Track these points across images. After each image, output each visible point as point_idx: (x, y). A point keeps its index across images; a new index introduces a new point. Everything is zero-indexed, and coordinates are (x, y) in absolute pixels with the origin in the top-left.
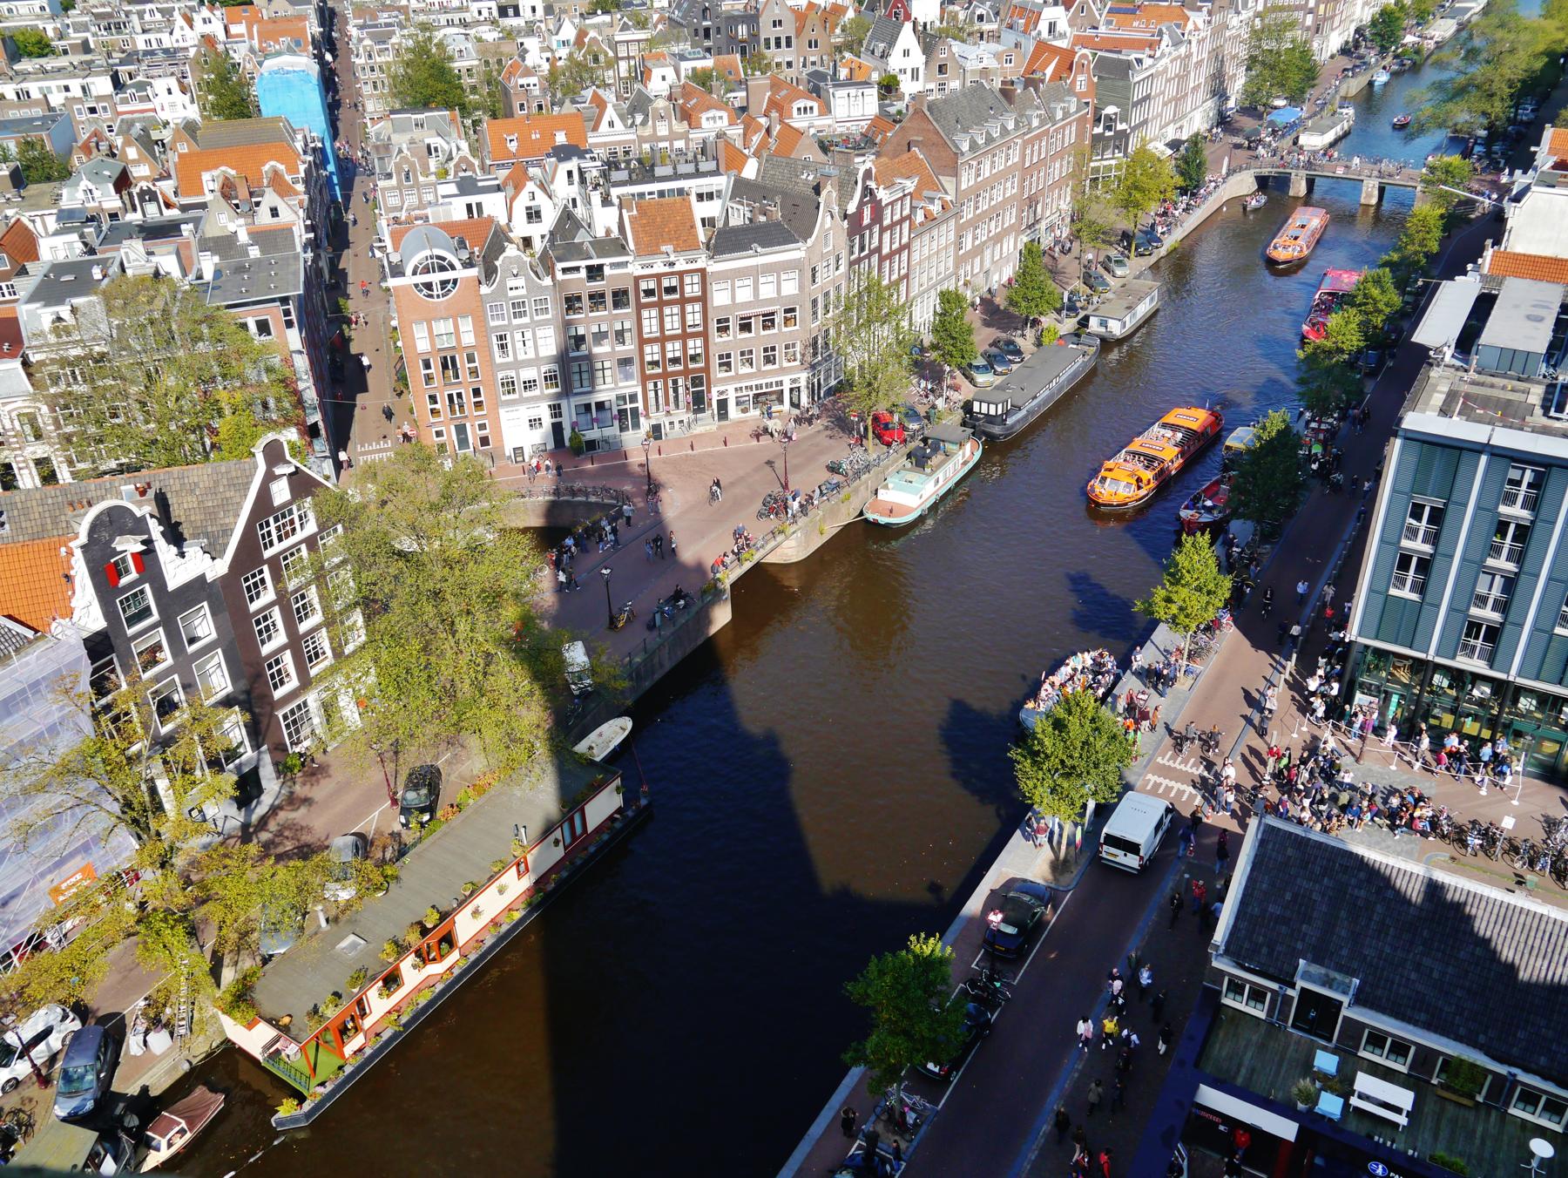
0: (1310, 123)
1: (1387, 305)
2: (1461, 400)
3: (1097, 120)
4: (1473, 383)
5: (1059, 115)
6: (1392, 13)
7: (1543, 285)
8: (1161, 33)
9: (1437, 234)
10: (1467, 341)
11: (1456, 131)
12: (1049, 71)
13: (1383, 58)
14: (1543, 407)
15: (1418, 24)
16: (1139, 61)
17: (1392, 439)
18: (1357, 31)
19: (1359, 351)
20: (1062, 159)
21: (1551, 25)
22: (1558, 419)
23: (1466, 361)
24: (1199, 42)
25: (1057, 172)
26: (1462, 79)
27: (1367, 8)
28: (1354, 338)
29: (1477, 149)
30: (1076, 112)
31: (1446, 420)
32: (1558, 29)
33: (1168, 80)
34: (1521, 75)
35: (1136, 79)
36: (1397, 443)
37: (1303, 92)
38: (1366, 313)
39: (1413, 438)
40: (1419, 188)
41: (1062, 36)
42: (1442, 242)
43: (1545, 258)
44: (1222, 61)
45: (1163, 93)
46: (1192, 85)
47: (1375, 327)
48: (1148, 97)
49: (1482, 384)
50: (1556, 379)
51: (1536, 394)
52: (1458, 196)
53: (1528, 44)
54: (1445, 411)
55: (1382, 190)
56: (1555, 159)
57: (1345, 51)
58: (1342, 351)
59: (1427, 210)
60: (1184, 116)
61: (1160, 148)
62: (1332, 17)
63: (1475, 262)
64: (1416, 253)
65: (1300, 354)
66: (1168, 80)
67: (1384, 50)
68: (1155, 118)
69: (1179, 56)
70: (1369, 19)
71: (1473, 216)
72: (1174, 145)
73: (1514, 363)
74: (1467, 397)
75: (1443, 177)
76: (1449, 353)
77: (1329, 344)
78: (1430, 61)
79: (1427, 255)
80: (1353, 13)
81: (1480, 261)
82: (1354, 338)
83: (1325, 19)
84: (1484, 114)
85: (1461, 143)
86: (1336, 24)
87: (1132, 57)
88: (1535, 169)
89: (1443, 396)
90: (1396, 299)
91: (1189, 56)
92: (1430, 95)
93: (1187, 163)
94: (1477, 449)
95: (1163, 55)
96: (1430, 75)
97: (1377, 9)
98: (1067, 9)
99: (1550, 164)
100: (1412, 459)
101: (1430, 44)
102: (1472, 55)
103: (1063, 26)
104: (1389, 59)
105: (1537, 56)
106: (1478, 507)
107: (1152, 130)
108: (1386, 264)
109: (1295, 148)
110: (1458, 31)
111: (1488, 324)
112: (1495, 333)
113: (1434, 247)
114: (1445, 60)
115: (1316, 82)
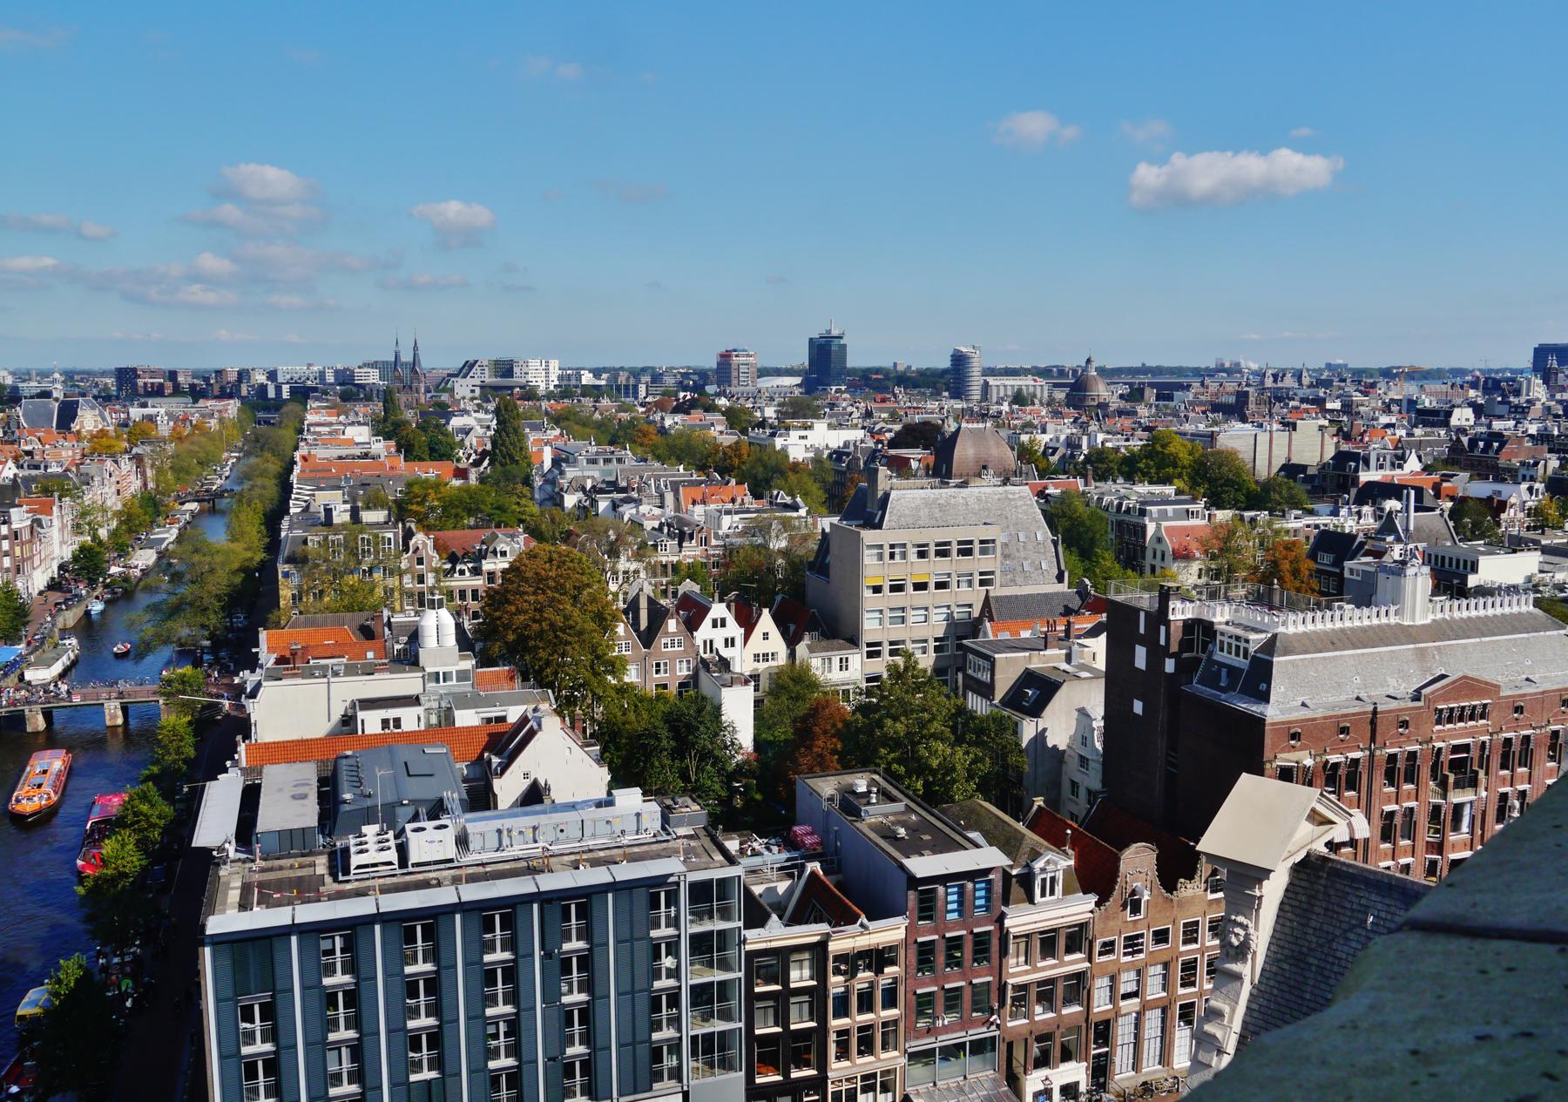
0: (32, 658)
1: (160, 817)
2: (256, 890)
4: (263, 870)
6: (90, 549)
7: (298, 766)
9: (190, 740)
10: (246, 831)
11: (181, 645)
13: (94, 589)
14: (331, 874)
15: (120, 556)
17: (200, 949)
18: (61, 567)
19: (143, 868)
22: (348, 881)
23: (251, 852)
26: (173, 599)
27: (64, 547)
28: (135, 859)
29: (206, 657)
31: (249, 913)
32: (246, 549)
34: (225, 590)
36: (207, 951)
38: (141, 830)
39: (221, 941)
40: (161, 702)
42: (197, 746)
43: (293, 742)
47: (154, 843)
49: (271, 869)
50: (335, 845)
51: (321, 865)
52: (199, 702)
53: (223, 564)
54: (244, 906)
55: (125, 709)
56: (275, 655)
57: (53, 586)
58: (125, 875)
59: (172, 720)
62: (31, 558)
63: (232, 759)
64: (175, 761)
65: (80, 890)
67: (92, 583)
70: (70, 556)
71: (219, 717)
73: (294, 842)
74: (261, 885)
75: (181, 687)
76: (231, 849)
77: (109, 872)
78: (140, 587)
79: (185, 761)
80: (53, 552)
81: (236, 756)
82: (135, 859)
83: (24, 560)
84: (203, 626)
85: (187, 654)
86: (36, 562)
88: (261, 667)
89: (238, 892)
90: (168, 810)
92: (147, 617)
94: (284, 932)
96: (144, 600)
97: (76, 547)
99: (272, 661)
100: (227, 962)
101: (137, 573)
102: (176, 577)
104: (100, 590)
105: (235, 573)
106: (304, 988)
108: (147, 779)
109: (22, 685)
110: (159, 559)
111: (260, 812)
112: (270, 818)
113: (191, 752)
114: (153, 585)
115: (29, 618)
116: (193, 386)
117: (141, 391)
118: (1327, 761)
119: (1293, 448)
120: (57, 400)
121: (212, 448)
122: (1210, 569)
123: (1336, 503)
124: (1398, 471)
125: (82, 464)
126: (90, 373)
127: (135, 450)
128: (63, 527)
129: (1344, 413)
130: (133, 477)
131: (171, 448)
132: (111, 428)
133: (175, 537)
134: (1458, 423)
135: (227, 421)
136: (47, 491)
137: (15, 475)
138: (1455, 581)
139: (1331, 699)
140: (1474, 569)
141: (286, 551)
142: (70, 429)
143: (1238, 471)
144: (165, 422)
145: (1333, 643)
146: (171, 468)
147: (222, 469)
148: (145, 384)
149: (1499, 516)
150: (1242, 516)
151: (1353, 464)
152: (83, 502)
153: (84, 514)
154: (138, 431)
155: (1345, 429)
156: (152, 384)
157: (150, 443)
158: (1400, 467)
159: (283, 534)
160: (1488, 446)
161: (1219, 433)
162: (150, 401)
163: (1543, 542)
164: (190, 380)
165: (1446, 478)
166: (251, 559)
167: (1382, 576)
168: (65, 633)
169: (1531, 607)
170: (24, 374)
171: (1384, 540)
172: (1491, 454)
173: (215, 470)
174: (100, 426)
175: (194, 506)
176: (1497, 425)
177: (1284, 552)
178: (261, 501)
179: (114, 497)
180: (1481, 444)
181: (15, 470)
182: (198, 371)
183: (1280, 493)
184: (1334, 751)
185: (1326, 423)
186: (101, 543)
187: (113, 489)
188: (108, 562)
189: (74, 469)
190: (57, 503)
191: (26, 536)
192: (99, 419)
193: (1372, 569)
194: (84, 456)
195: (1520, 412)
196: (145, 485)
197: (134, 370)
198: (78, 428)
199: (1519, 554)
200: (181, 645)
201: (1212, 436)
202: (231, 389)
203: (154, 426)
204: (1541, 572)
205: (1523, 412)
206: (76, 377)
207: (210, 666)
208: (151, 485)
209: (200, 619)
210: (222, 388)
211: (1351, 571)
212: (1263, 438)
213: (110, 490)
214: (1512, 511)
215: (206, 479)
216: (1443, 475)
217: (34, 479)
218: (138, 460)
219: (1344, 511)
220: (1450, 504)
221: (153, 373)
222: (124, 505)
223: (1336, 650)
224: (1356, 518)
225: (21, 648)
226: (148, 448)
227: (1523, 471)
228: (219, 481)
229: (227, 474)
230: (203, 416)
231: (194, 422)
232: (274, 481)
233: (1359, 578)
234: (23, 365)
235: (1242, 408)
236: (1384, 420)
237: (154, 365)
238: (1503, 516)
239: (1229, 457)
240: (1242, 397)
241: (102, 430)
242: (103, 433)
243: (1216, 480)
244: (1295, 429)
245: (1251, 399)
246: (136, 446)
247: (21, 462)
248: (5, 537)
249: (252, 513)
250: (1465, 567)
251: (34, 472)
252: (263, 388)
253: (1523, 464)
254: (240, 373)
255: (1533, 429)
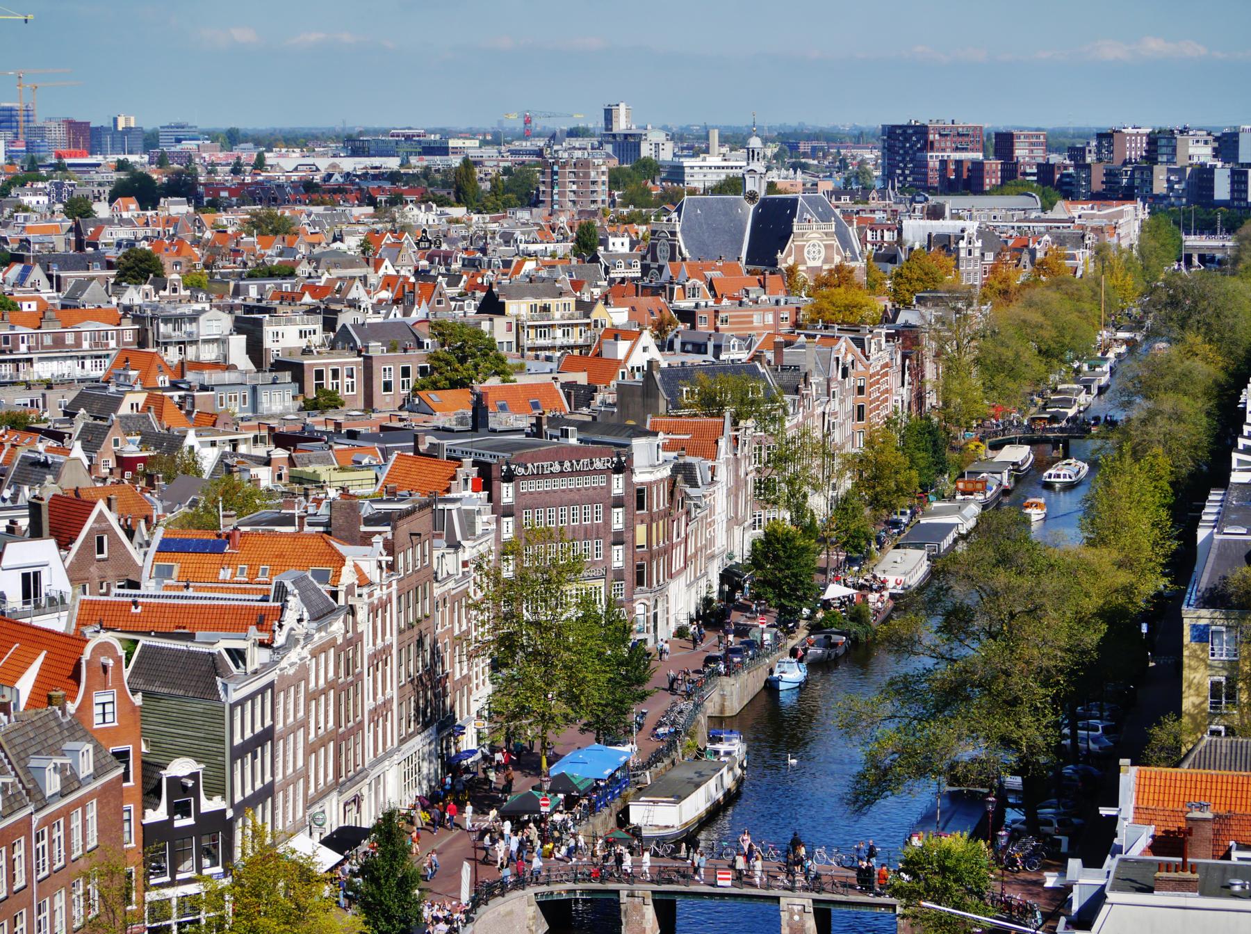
0: (648, 777)
3: (151, 794)
5: (53, 783)
6: (788, 539)
8: (282, 593)
12: (26, 684)
16: (238, 656)
20: (70, 889)
21: (1104, 557)
24: (373, 610)
25: (60, 918)
26: (944, 671)
27: (737, 531)
30: (95, 777)
32: (1120, 565)
33: (312, 696)
35: (235, 696)
37: (620, 709)
41: (56, 603)
44: (435, 652)
45: (304, 724)
46: (369, 704)
48: (267, 735)
60: (361, 774)
61: (305, 846)
62: (667, 551)
66: (312, 696)
68: (289, 782)
69: (332, 643)
72: (342, 840)
83: (652, 555)
87: (221, 647)
91: (354, 641)
92: (888, 708)
93: (374, 880)
95: (292, 641)
96: (889, 666)
97: (759, 533)
98: (64, 545)
103: (55, 581)
107: (289, 808)
110: (933, 574)
115: (647, 687)
116: (1045, 171)
117: (934, 179)
120: (752, 197)
121: (1073, 317)
125: (789, 344)
126: (831, 137)
127: (904, 317)
128: (734, 493)
130: (894, 380)
131: (980, 315)
132: (860, 264)
133: (971, 523)
135: (1113, 254)
136: (711, 404)
137: (650, 363)
141: (1204, 578)
142: (775, 263)
144: (977, 253)
146: (977, 361)
147: (1092, 368)
148: (944, 163)
152: (783, 431)
153: (780, 460)
154: (918, 273)
156: (959, 163)
157: (938, 301)
159: (1202, 534)
162: (951, 203)
164: (1040, 156)
166: (1128, 590)
168: (720, 725)
170: (698, 138)
173: (1078, 371)
174: (837, 259)
175: (1020, 454)
178: (1169, 452)
179: (850, 425)
181: (654, 353)
182: (1063, 133)
186: (809, 530)
187: (849, 404)
188: (824, 571)
189: (770, 355)
190: (729, 431)
191: (659, 501)
192: (836, 243)
194: (797, 325)
196: (920, 398)
197: (922, 131)
198: (791, 261)
200: (954, 780)
202: (1132, 177)
203: (950, 262)
206: (804, 147)
207: (1014, 837)
208: (932, 400)
209: (1005, 726)
210: (1111, 175)
213: (841, 407)
215: (1055, 391)
217: (683, 373)
218: (908, 338)
221: (962, 138)
222: (869, 443)
225: (628, 751)
226: (931, 313)
228: (1083, 398)
229: (1104, 380)
230: (1060, 241)
231: (1040, 255)
232: (1203, 404)
234: (693, 120)
237: (966, 120)
241: (839, 269)
242: (841, 276)
246: (908, 306)
247: (670, 335)
248: (618, 502)
249: (1142, 478)
251: (696, 359)
252: (1204, 176)
254: (1153, 141)
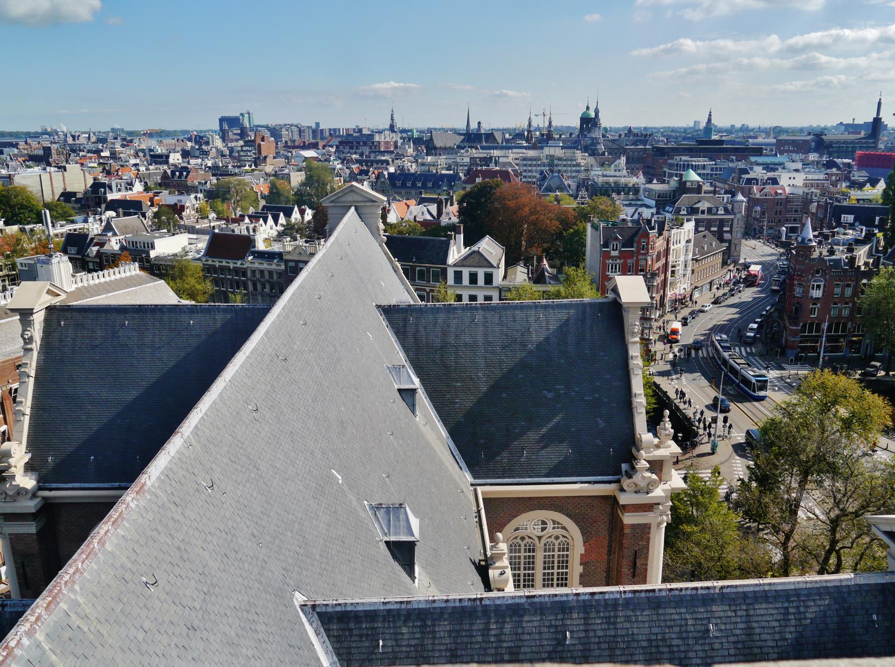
118: (11, 389)
119: (66, 182)
122: (6, 265)
123: (88, 214)
124: (130, 192)
129: (111, 158)
134: (173, 162)
138: (144, 255)
139: (8, 349)
140: (153, 247)
143: (28, 199)
145: (6, 313)
149: (181, 214)
150: (24, 228)
151: (102, 190)
155: (107, 168)
158: (131, 189)
160: (181, 174)
161: (14, 175)
163: (197, 227)
165: (157, 194)
167: (39, 265)
169: (138, 272)
171: (106, 235)
172: (183, 178)
176: (193, 161)
177: (43, 250)
180: (177, 173)
183: (57, 211)
184: (14, 381)
185: (96, 165)
193: (32, 262)
195: (206, 154)
199: (176, 236)
201: (10, 177)
204: (190, 244)
205: (206, 154)
211: (21, 264)
212: (45, 177)
214: (188, 210)
216: (155, 193)
219: (91, 219)
220: (155, 209)
223: (8, 317)
224: (99, 223)
227: (200, 187)
233: (27, 269)
235: (48, 157)
236: (133, 161)
238: (184, 214)
239: (23, 189)
240: (47, 150)
243: (15, 206)
244: (65, 170)
245: (53, 152)
250: (148, 247)
253: (200, 183)
255: (210, 164)
